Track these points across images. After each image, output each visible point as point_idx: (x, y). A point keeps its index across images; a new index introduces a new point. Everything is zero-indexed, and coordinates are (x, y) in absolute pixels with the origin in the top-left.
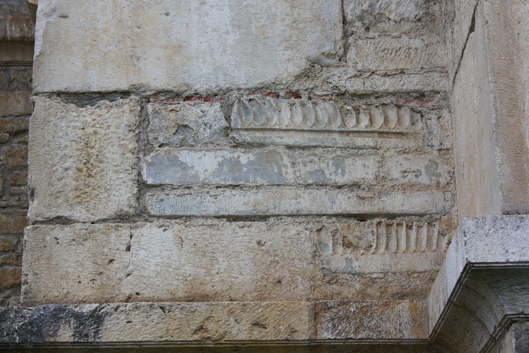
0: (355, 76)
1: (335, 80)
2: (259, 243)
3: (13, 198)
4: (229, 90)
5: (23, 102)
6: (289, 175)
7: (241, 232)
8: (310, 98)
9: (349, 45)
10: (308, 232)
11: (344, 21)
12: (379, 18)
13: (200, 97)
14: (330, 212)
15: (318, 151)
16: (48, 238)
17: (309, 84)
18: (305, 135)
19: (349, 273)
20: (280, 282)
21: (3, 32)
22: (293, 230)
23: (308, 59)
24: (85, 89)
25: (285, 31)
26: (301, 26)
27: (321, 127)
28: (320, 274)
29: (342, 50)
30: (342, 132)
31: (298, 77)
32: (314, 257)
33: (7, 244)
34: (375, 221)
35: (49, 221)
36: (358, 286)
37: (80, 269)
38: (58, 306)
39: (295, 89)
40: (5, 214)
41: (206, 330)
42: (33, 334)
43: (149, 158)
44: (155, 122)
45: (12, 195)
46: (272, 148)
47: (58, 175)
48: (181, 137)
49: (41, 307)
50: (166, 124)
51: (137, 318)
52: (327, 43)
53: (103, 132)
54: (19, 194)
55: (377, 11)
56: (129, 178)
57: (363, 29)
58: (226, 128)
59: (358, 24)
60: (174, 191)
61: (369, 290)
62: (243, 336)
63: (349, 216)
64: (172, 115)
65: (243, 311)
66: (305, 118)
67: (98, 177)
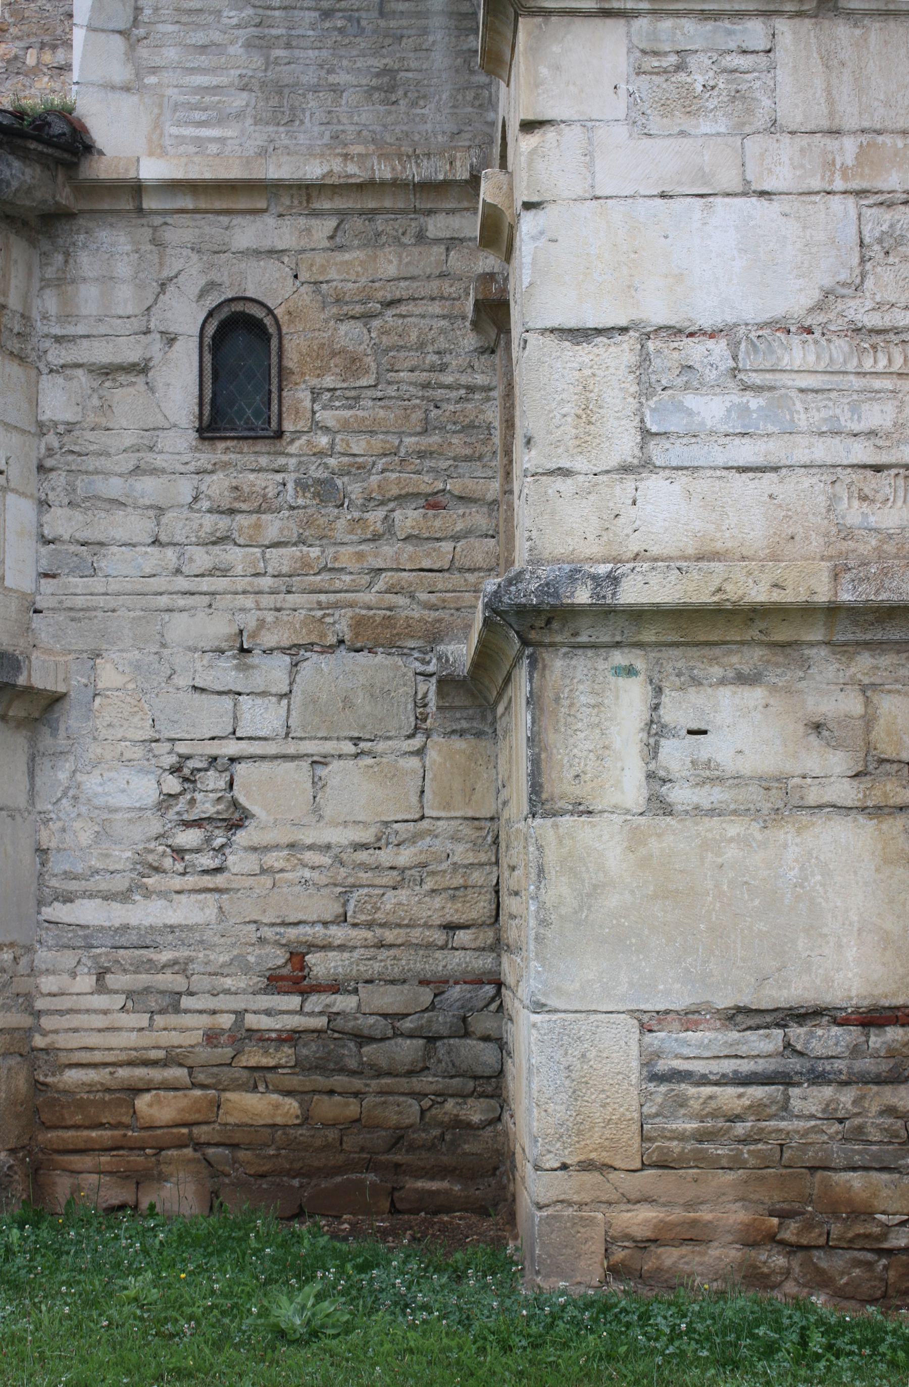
0: (874, 309)
1: (851, 314)
2: (770, 496)
3: (390, 387)
4: (736, 325)
5: (395, 263)
6: (802, 422)
7: (752, 485)
8: (823, 334)
9: (867, 273)
10: (822, 485)
11: (862, 244)
12: (900, 241)
13: (705, 334)
14: (845, 462)
15: (833, 395)
16: (550, 491)
17: (822, 318)
18: (819, 376)
19: (865, 528)
20: (792, 538)
21: (370, 172)
22: (806, 482)
23: (821, 289)
24: (580, 325)
25: (796, 256)
26: (814, 250)
27: (836, 368)
28: (834, 530)
29: (859, 278)
30: (859, 373)
31: (811, 310)
32: (829, 511)
33: (388, 446)
34: (893, 472)
35: (550, 473)
36: (874, 543)
37: (585, 524)
38: (573, 566)
39: (806, 324)
40: (382, 407)
41: (725, 592)
42: (549, 595)
43: (652, 403)
44: (657, 363)
45: (389, 383)
46: (783, 391)
47: (556, 421)
48: (685, 379)
49: (556, 567)
50: (669, 365)
51: (655, 579)
52: (842, 271)
53: (602, 374)
54: (397, 383)
55: (898, 233)
57: (882, 254)
58: (735, 369)
59: (876, 247)
60: (680, 440)
61: (885, 546)
62: (762, 598)
63: (865, 467)
64: (675, 354)
65: (762, 571)
66: (818, 358)
67: (598, 424)
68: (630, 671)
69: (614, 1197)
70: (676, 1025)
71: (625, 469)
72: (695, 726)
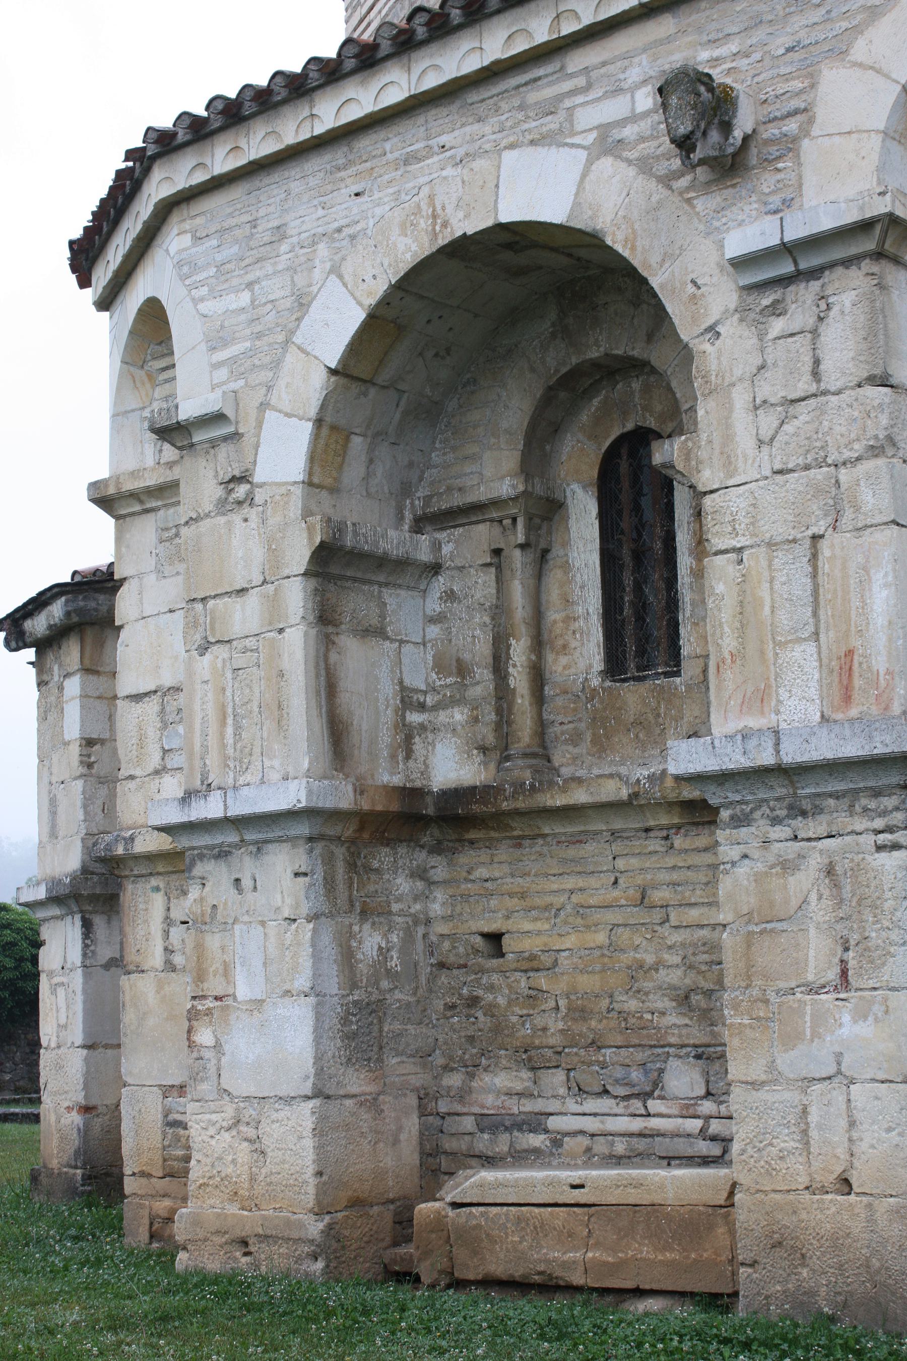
56: (157, 746)
68: (157, 889)
69: (154, 1193)
70: (175, 1094)
71: (157, 772)
72: (183, 919)
